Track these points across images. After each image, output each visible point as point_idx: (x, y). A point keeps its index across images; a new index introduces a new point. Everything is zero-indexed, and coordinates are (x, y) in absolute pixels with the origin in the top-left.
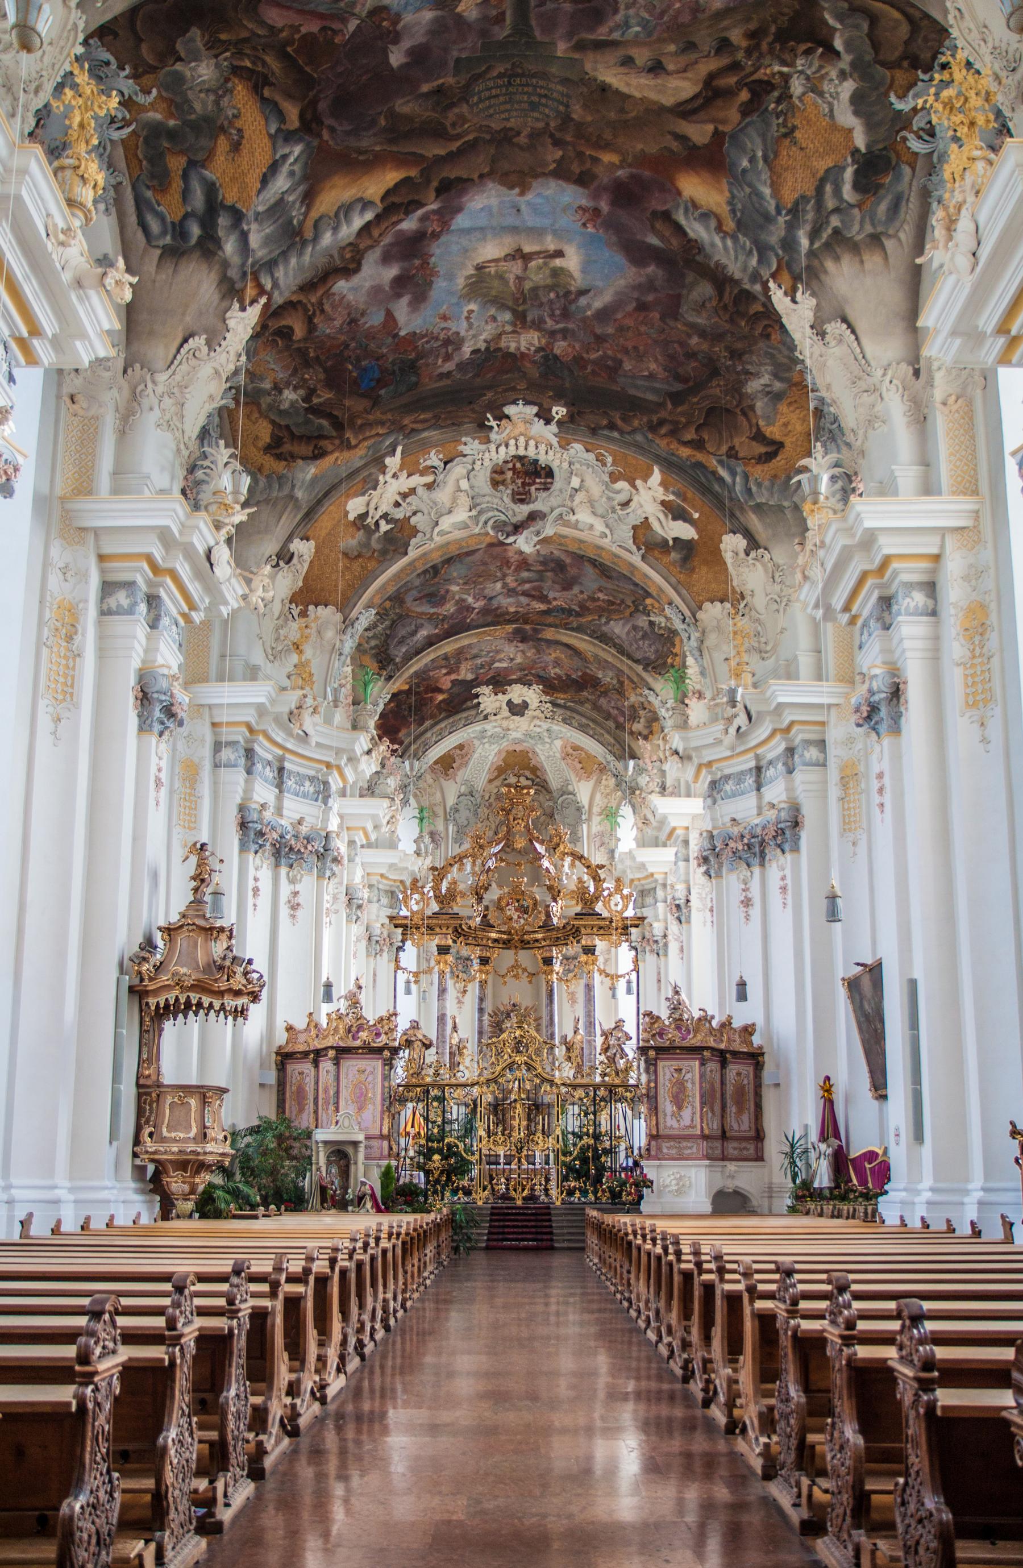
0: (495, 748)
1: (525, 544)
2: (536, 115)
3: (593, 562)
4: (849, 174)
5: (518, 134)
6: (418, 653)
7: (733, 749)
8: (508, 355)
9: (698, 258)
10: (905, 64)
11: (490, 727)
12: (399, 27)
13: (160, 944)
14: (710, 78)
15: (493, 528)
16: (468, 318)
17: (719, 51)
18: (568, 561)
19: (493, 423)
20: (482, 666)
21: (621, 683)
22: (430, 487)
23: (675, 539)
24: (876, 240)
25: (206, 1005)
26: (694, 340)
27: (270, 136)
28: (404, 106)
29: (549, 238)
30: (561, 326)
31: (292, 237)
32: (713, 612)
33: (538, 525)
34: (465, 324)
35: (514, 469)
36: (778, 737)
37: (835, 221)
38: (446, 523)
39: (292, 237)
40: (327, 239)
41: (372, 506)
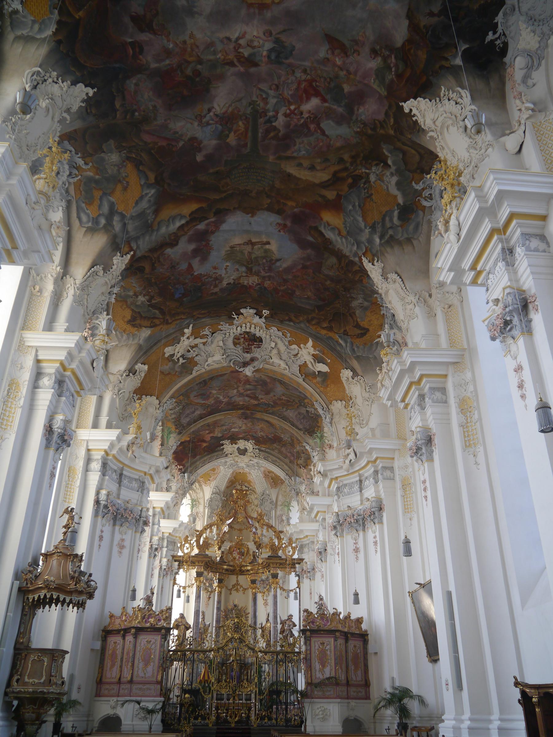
0: (231, 471)
1: (248, 371)
3: (281, 382)
4: (396, 213)
6: (195, 421)
7: (348, 471)
8: (243, 286)
9: (330, 246)
10: (418, 171)
11: (229, 460)
13: (41, 563)
14: (335, 174)
15: (233, 364)
16: (226, 269)
18: (268, 381)
19: (235, 316)
20: (226, 430)
21: (292, 440)
22: (204, 344)
23: (318, 372)
24: (409, 240)
25: (61, 599)
26: (328, 282)
27: (141, 185)
29: (264, 236)
30: (268, 274)
31: (148, 228)
32: (337, 406)
33: (256, 363)
34: (224, 271)
35: (244, 338)
36: (370, 465)
37: (390, 232)
38: (210, 360)
39: (148, 228)
40: (163, 230)
41: (177, 351)
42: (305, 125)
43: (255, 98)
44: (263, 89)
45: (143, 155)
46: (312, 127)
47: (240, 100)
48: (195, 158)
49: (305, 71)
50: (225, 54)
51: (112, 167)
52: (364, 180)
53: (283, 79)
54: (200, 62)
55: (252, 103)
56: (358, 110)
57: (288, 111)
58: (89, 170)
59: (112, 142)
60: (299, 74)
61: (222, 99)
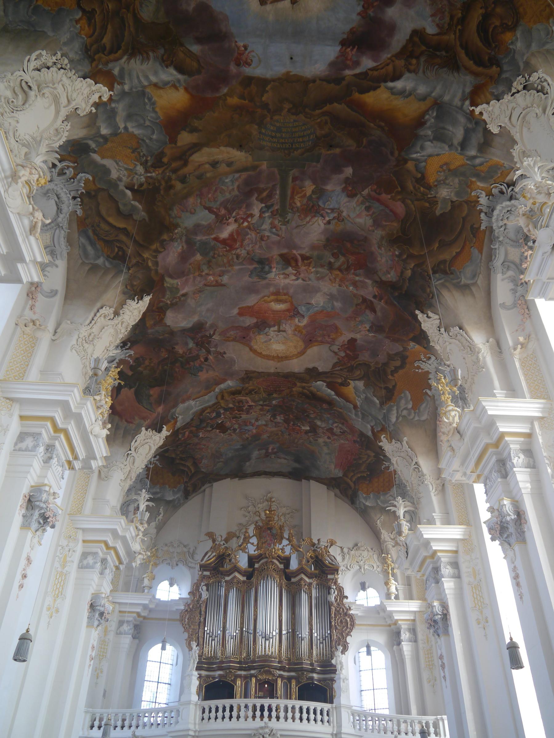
2: (278, 125)
5: (289, 111)
12: (344, 185)
14: (186, 164)
17: (185, 177)
28: (351, 144)
40: (422, 90)
42: (230, 212)
43: (284, 227)
44: (275, 236)
45: (412, 188)
46: (223, 212)
47: (297, 227)
48: (353, 172)
49: (238, 256)
50: (309, 271)
51: (451, 184)
52: (149, 164)
53: (257, 247)
54: (330, 266)
55: (286, 223)
56: (183, 247)
57: (249, 220)
58: (479, 188)
59: (438, 212)
60: (243, 253)
61: (315, 230)
